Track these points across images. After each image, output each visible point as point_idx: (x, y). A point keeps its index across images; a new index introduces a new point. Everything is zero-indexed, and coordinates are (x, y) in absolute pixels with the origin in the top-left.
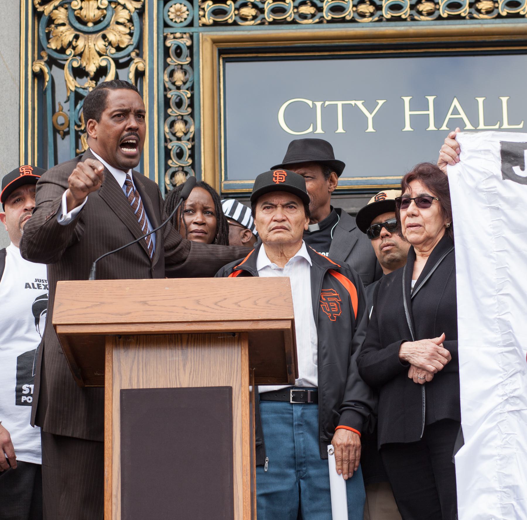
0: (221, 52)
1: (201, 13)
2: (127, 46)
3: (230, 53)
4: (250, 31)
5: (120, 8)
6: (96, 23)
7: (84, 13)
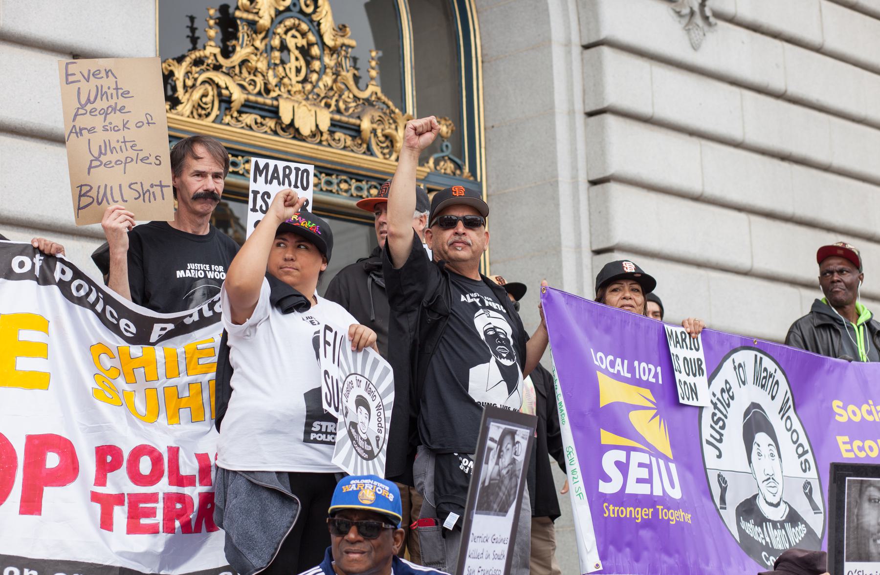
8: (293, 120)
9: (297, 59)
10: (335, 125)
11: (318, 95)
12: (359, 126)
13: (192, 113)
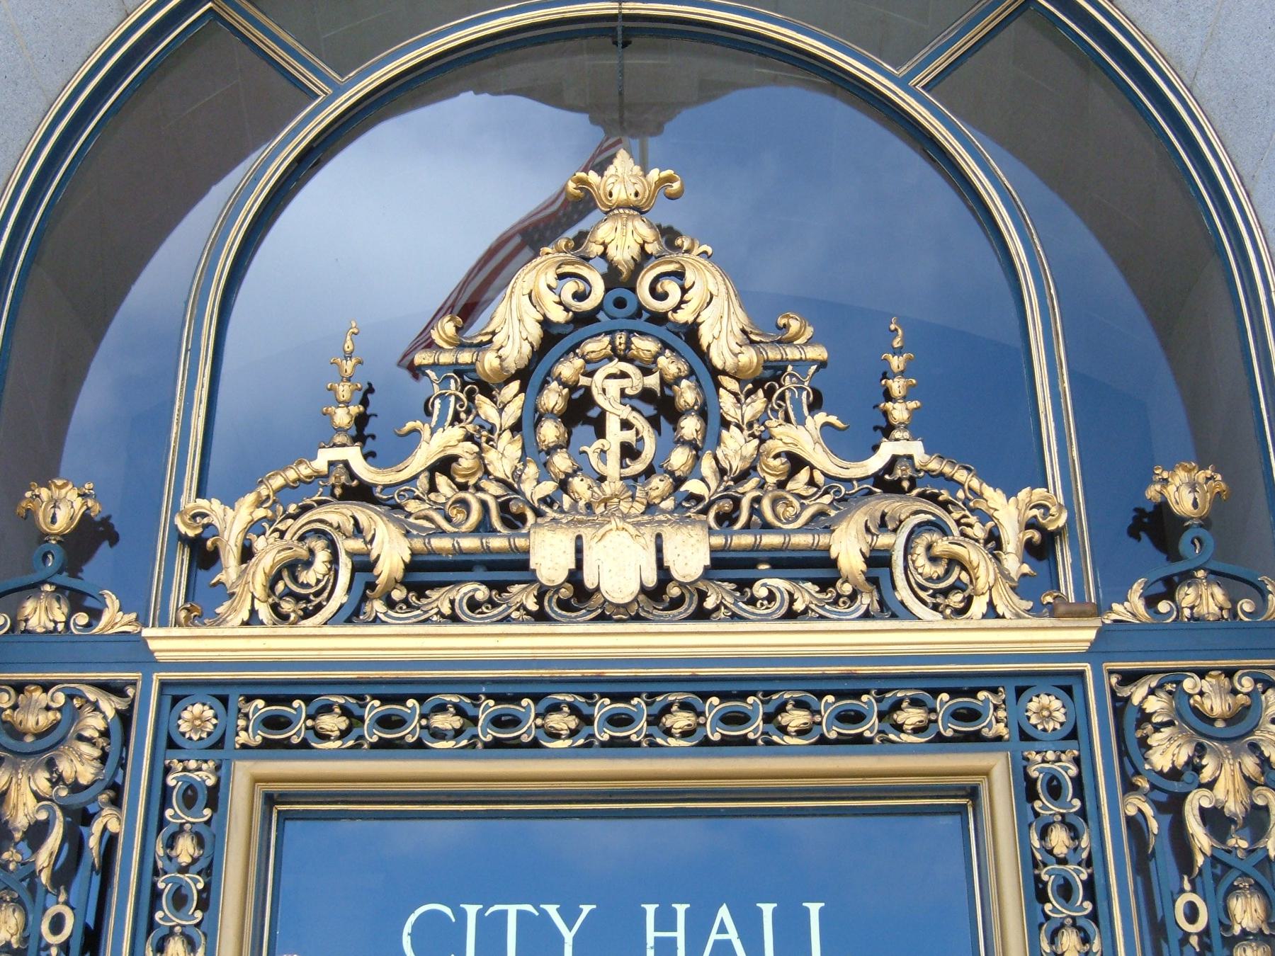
0: (270, 800)
1: (242, 723)
2: (93, 783)
5: (88, 709)
6: (39, 735)
7: (18, 716)
8: (575, 577)
9: (626, 425)
11: (699, 499)
12: (828, 549)
13: (253, 612)
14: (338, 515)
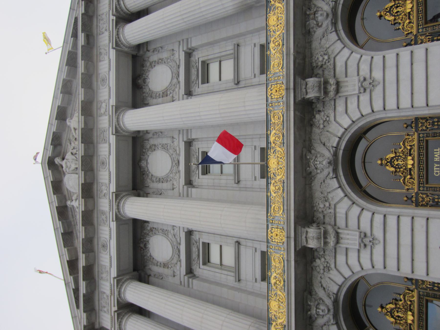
3: (427, 183)
4: (425, 180)
10: (410, 155)
14: (406, 180)
